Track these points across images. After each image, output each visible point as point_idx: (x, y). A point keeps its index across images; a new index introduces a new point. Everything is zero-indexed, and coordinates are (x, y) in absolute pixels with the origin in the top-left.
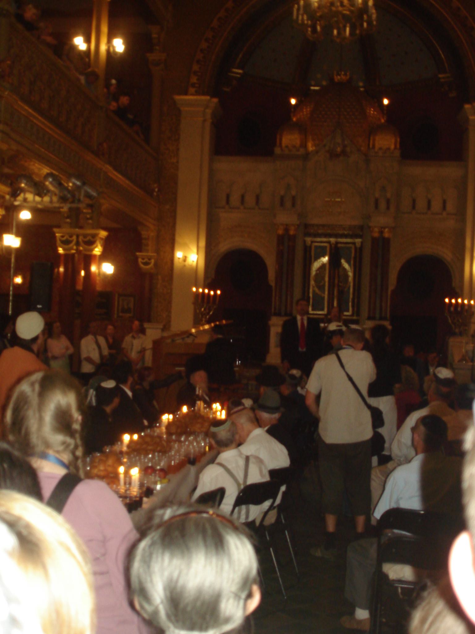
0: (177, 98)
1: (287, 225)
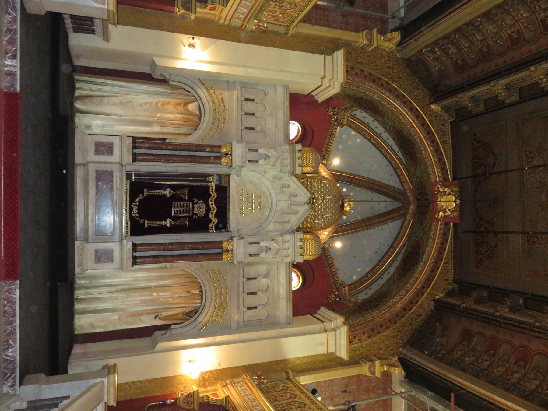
1: (231, 155)
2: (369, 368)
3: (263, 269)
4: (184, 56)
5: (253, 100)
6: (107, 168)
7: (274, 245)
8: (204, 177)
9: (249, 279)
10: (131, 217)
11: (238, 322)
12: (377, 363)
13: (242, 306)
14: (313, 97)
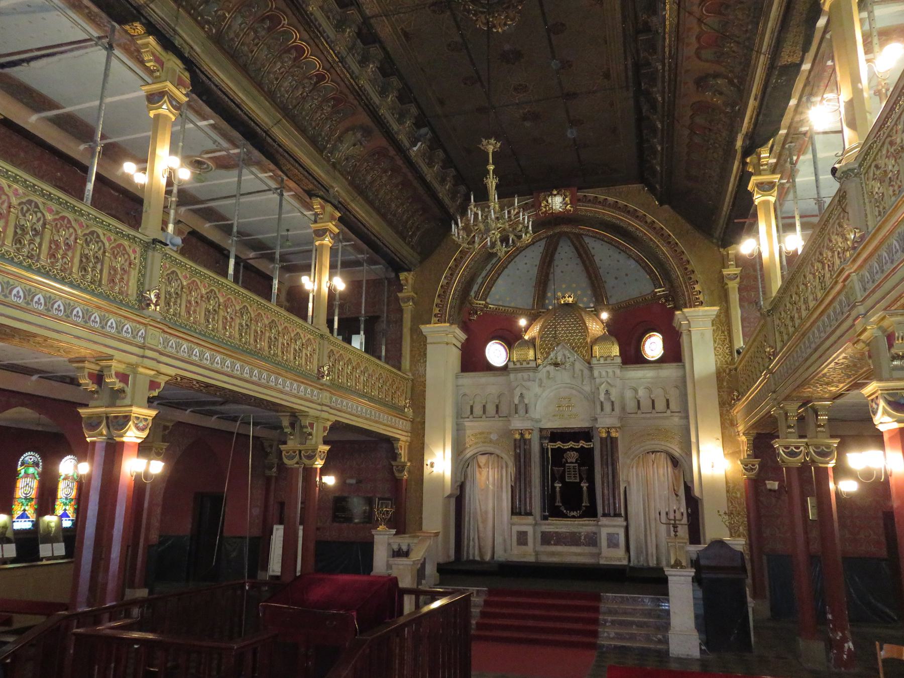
0: (422, 327)
2: (731, 279)
3: (629, 394)
4: (441, 472)
5: (472, 407)
6: (539, 536)
7: (603, 388)
8: (543, 451)
9: (639, 408)
10: (580, 517)
11: (681, 418)
12: (725, 272)
13: (665, 415)
14: (463, 345)
